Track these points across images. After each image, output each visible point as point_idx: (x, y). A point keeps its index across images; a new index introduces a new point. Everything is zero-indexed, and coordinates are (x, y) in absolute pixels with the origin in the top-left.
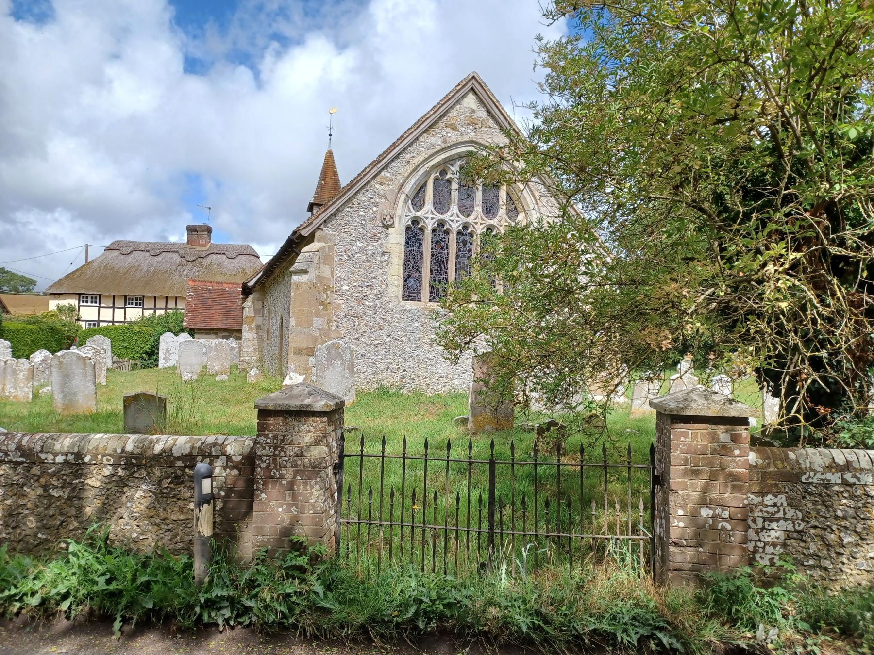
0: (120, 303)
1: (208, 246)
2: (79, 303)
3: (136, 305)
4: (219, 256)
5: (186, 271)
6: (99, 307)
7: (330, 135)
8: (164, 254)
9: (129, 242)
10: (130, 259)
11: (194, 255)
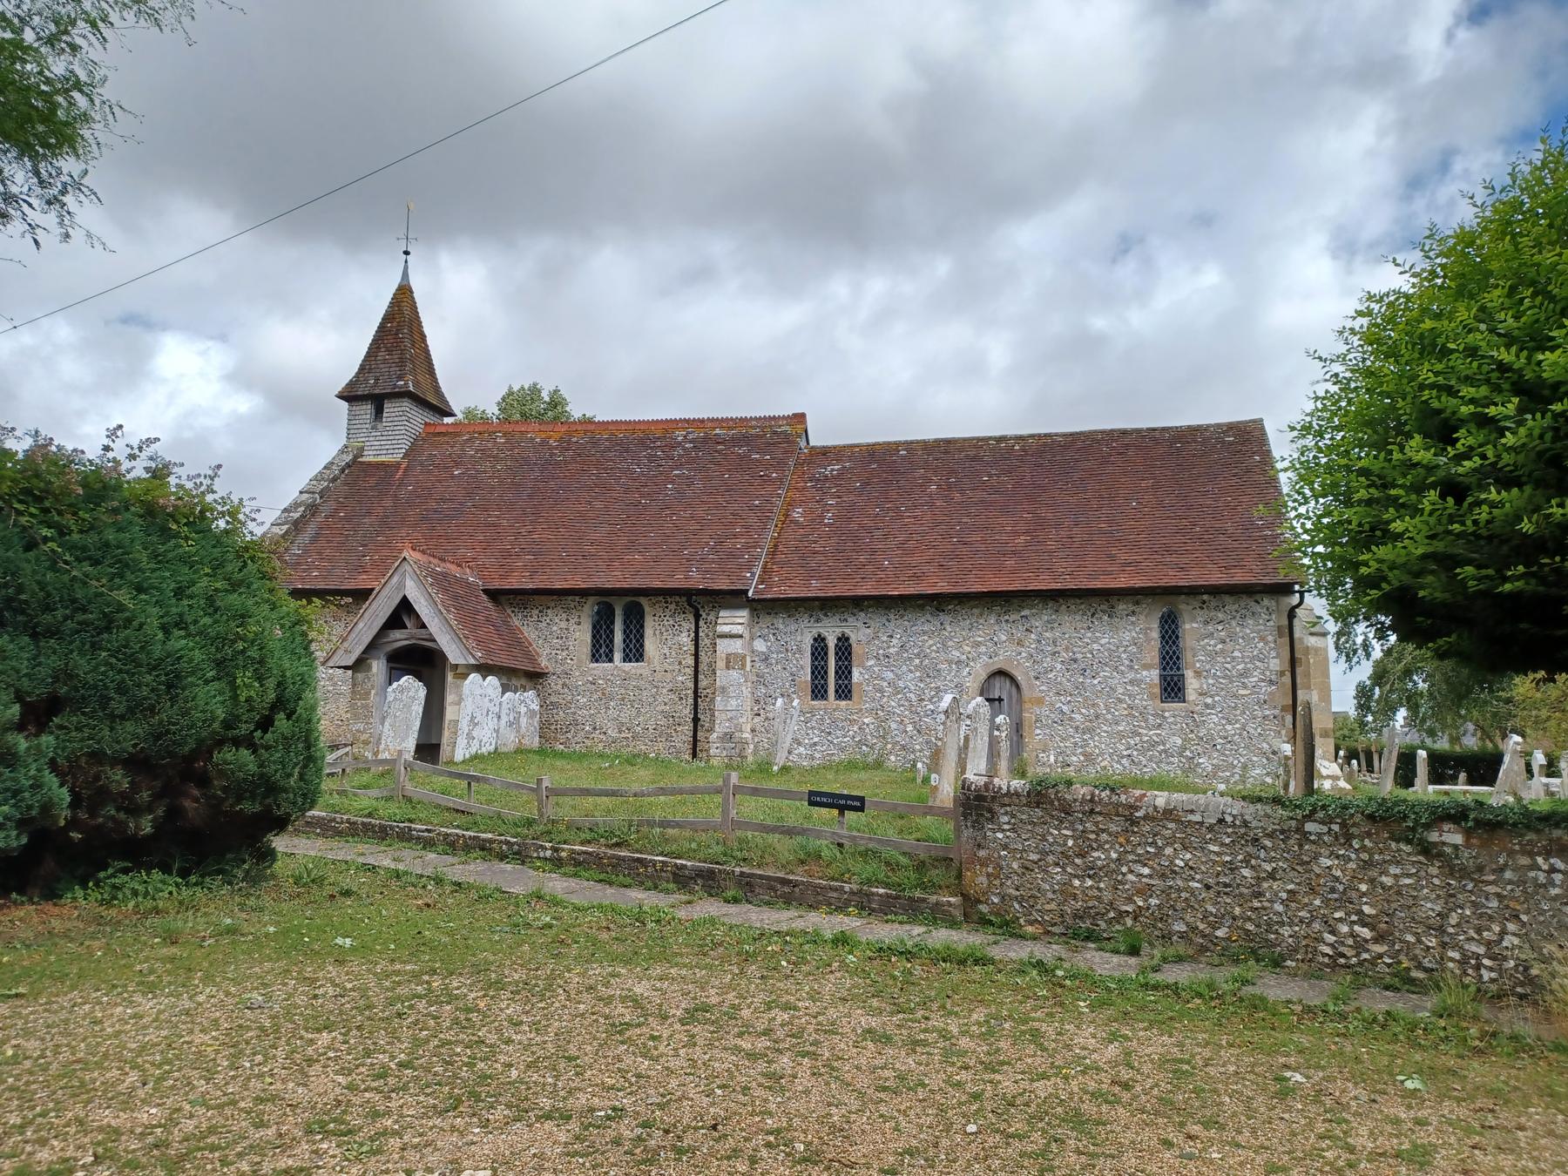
7: (407, 253)
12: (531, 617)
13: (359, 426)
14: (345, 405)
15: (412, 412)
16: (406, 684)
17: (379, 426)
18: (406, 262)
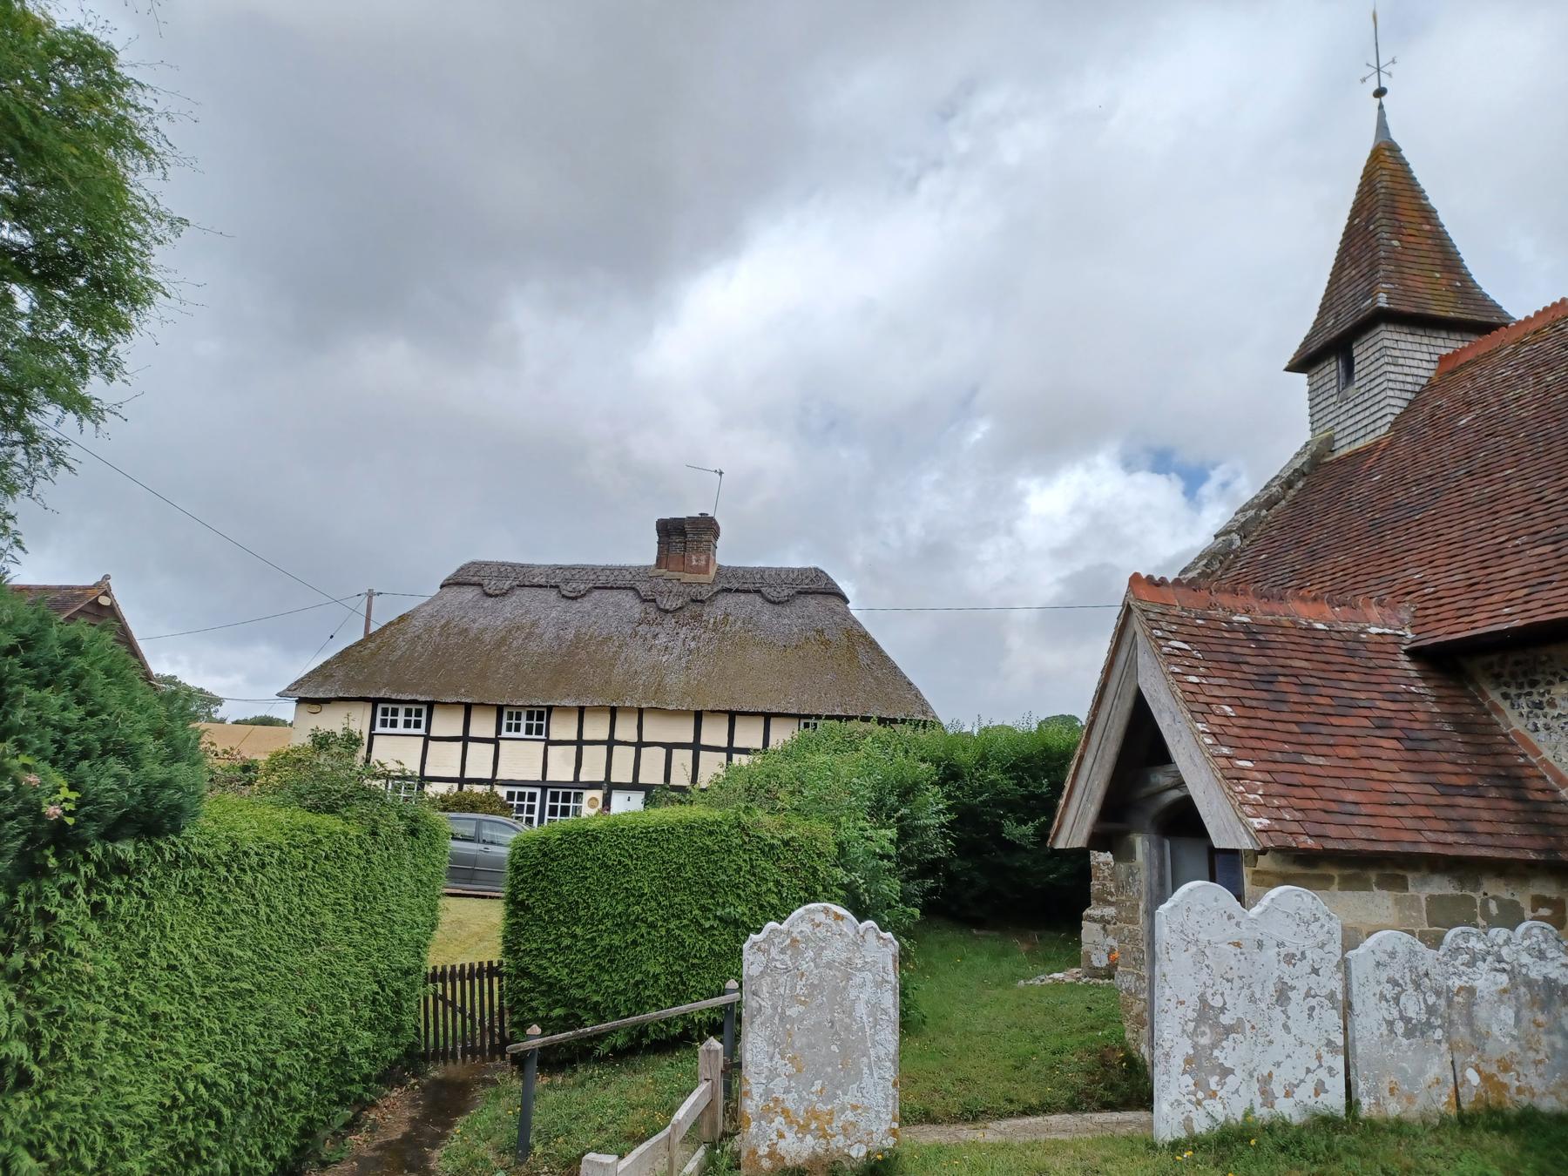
0: (483, 725)
1: (712, 572)
2: (372, 727)
3: (529, 731)
4: (743, 597)
5: (662, 639)
6: (428, 738)
8: (596, 593)
9: (503, 564)
10: (509, 608)
11: (679, 595)
12: (1552, 704)
13: (1323, 405)
14: (1302, 378)
15: (1402, 345)
16: (806, 928)
17: (1351, 391)
18: (1381, 107)
